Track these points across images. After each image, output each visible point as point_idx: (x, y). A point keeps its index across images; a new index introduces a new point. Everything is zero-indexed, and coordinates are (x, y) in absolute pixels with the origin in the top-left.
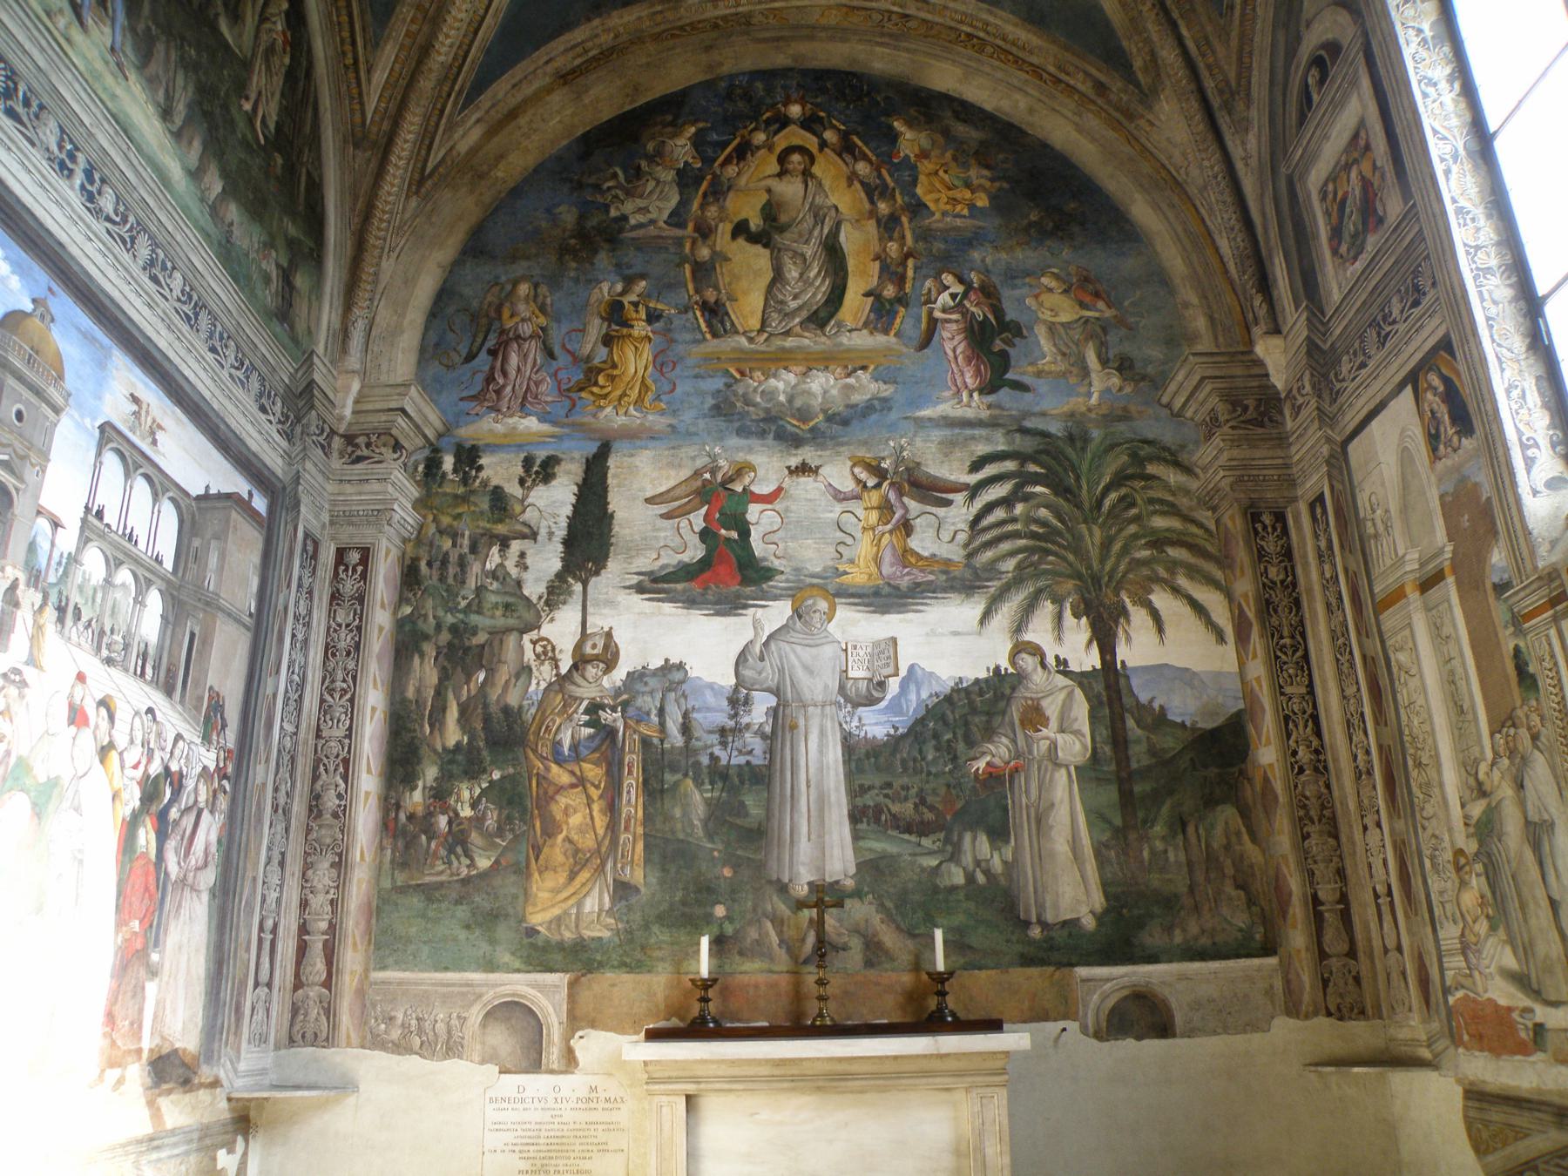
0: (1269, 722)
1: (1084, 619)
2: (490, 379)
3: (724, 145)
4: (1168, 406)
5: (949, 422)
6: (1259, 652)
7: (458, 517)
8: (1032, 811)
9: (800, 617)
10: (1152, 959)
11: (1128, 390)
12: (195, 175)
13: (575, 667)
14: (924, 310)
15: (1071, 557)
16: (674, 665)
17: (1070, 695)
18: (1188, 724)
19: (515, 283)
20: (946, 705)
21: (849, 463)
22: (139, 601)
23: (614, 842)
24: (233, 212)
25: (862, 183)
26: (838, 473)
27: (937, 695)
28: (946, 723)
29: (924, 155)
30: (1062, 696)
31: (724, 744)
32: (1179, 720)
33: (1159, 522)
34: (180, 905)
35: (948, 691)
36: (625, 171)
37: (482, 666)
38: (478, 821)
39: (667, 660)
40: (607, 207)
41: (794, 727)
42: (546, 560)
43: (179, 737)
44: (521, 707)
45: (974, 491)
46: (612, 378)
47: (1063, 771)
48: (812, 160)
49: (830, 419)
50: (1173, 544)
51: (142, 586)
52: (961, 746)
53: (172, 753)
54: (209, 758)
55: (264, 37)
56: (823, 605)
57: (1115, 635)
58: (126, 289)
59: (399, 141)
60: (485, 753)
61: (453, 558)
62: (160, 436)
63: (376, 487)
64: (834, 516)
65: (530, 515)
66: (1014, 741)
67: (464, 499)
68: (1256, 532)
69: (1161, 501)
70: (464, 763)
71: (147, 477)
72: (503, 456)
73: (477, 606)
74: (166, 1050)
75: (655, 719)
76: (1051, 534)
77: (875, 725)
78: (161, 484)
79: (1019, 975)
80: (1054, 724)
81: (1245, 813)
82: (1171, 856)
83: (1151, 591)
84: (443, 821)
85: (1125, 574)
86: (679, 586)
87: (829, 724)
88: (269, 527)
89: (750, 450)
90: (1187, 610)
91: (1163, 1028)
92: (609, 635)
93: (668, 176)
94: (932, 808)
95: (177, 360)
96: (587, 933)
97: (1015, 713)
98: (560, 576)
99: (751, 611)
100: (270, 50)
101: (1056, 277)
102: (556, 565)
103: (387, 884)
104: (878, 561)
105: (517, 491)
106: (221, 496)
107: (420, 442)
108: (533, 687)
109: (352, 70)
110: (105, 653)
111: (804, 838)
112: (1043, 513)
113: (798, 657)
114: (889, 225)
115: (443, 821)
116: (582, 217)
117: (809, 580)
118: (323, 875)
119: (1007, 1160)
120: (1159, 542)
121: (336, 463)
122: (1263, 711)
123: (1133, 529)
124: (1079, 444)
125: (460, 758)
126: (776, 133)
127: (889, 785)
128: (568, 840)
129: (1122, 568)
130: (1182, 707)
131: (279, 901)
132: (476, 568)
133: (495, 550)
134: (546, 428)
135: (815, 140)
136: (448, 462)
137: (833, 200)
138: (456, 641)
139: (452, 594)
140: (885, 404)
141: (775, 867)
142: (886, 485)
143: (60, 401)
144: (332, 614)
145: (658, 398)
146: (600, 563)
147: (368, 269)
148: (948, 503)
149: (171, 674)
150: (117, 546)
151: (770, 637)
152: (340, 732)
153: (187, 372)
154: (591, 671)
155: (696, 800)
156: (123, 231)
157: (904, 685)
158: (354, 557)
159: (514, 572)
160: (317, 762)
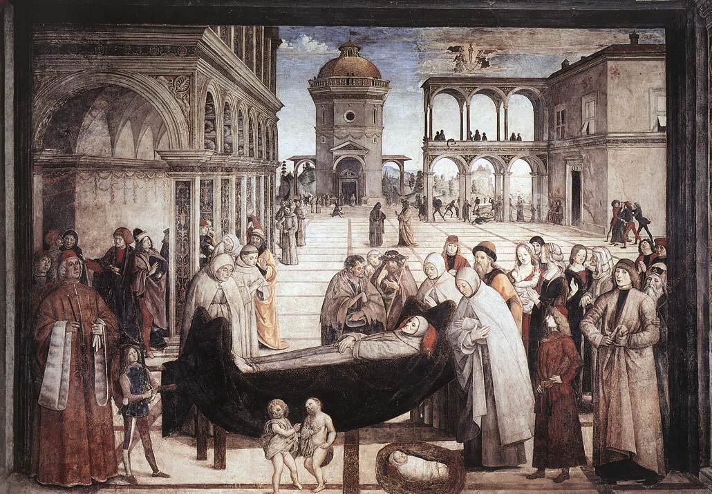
34: (611, 362)
53: (572, 261)
106: (584, 60)
110: (473, 217)
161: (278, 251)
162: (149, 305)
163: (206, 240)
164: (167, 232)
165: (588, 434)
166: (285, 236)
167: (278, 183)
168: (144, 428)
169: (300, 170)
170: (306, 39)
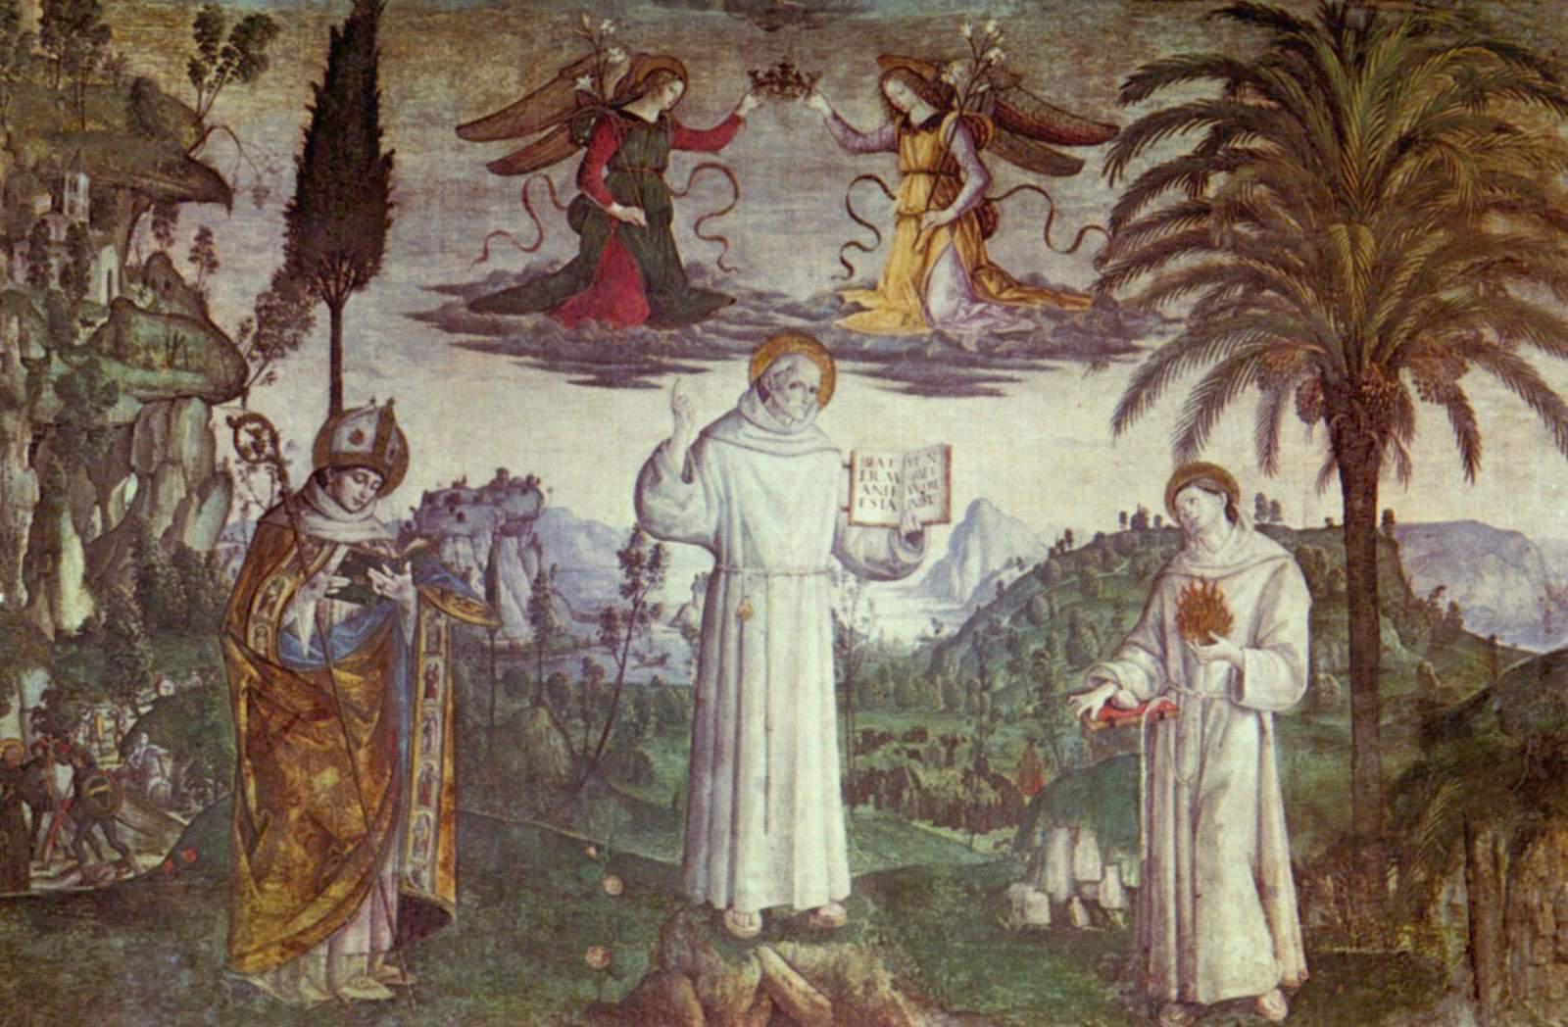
8: (1185, 792)
9: (764, 396)
13: (318, 477)
16: (514, 484)
20: (1038, 585)
21: (879, 71)
27: (1020, 563)
28: (1033, 620)
30: (1265, 572)
33: (1497, 225)
35: (1042, 556)
37: (132, 469)
39: (501, 472)
44: (211, 555)
47: (1251, 723)
56: (810, 372)
57: (1378, 460)
66: (1163, 659)
83: (1461, 370)
84: (63, 776)
86: (527, 321)
92: (386, 417)
94: (997, 782)
96: (349, 992)
99: (668, 380)
102: (275, 259)
108: (234, 518)
113: (756, 474)
115: (63, 776)
117: (783, 320)
125: (90, 652)
127: (919, 734)
128: (313, 818)
138: (72, 415)
141: (701, 882)
148: (1074, 167)
151: (705, 434)
154: (352, 488)
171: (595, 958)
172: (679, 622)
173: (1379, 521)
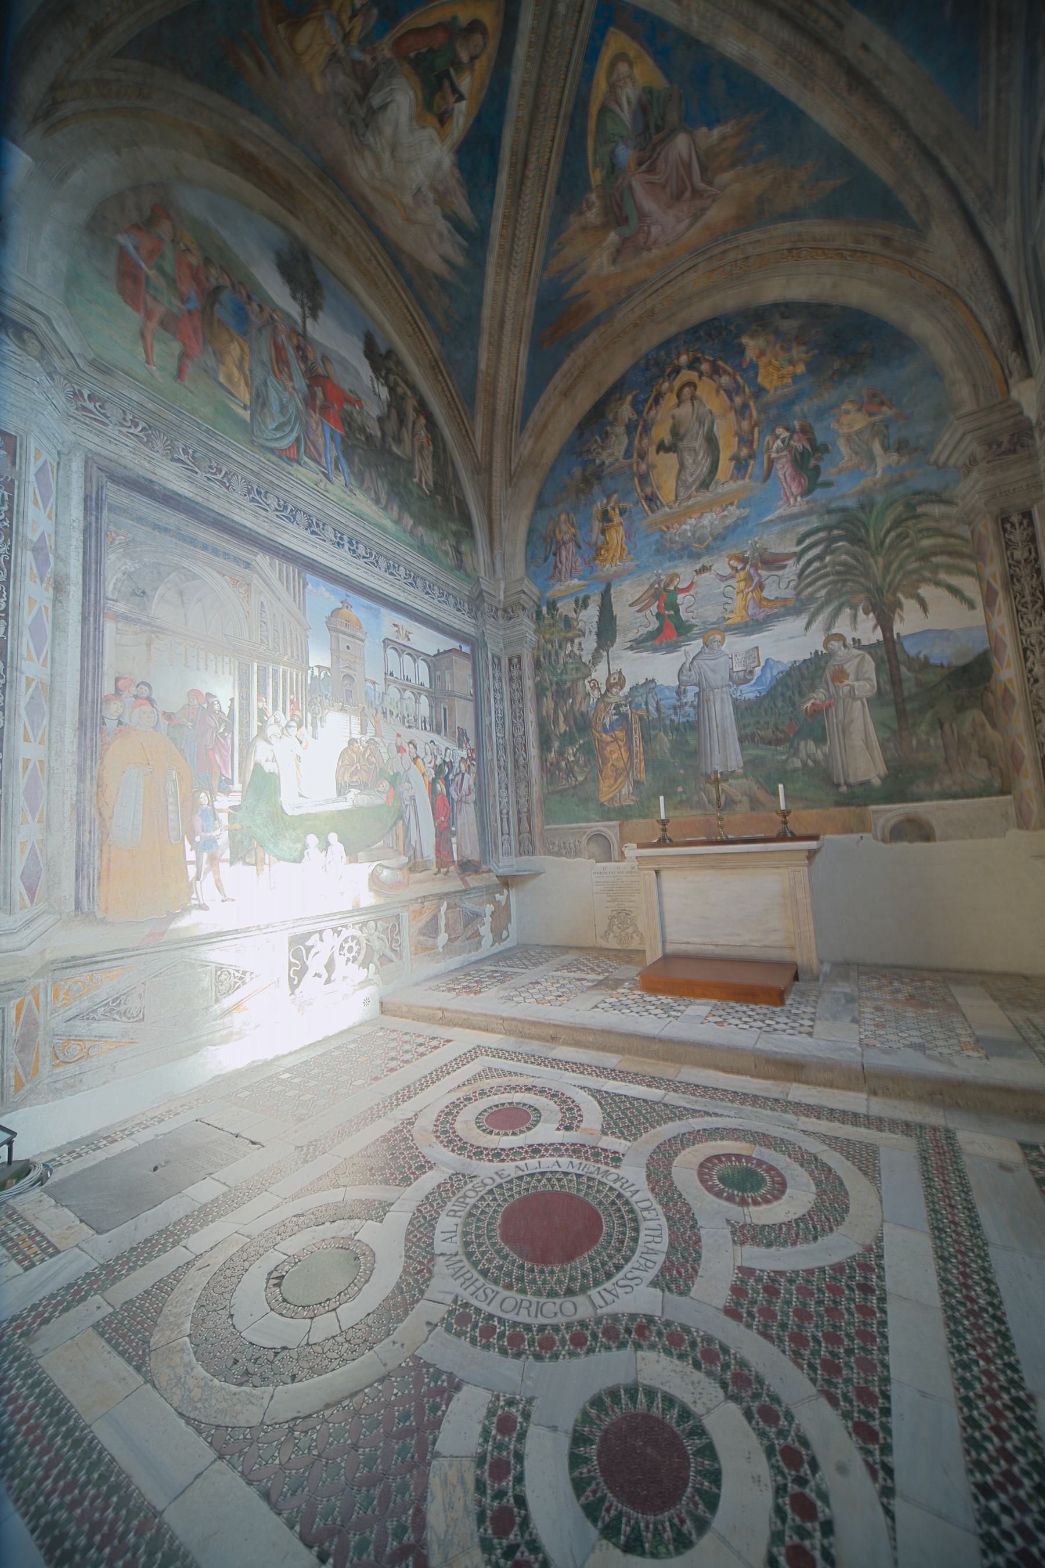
0: (1010, 652)
1: (871, 615)
2: (556, 566)
3: (646, 400)
4: (936, 463)
5: (782, 519)
6: (1003, 608)
7: (552, 634)
8: (840, 727)
10: (920, 799)
11: (904, 461)
12: (398, 522)
13: (607, 690)
14: (765, 457)
15: (862, 580)
17: (863, 659)
18: (945, 664)
19: (559, 516)
22: (417, 701)
23: (632, 764)
24: (421, 530)
25: (726, 391)
26: (721, 566)
29: (762, 354)
30: (857, 660)
31: (676, 714)
32: (938, 662)
33: (926, 543)
36: (600, 437)
38: (576, 762)
40: (594, 460)
41: (708, 701)
42: (590, 643)
43: (447, 748)
45: (799, 556)
46: (607, 550)
47: (859, 702)
48: (695, 387)
49: (715, 539)
50: (936, 554)
51: (417, 696)
52: (797, 697)
54: (464, 754)
55: (417, 444)
56: (718, 637)
58: (380, 583)
59: (494, 464)
60: (577, 735)
61: (553, 652)
62: (410, 636)
63: (518, 628)
64: (721, 590)
65: (581, 625)
66: (828, 691)
67: (554, 625)
68: (1005, 530)
69: (928, 529)
70: (568, 739)
71: (409, 654)
72: (566, 601)
73: (565, 671)
74: (465, 860)
75: (643, 706)
76: (848, 568)
77: (749, 692)
78: (416, 655)
79: (834, 811)
80: (852, 677)
81: (988, 713)
82: (932, 742)
83: (919, 587)
84: (563, 764)
85: (899, 582)
86: (649, 644)
87: (725, 696)
88: (473, 658)
89: (676, 567)
90: (945, 593)
91: (927, 836)
92: (620, 672)
93: (620, 430)
94: (782, 732)
95: (411, 604)
96: (624, 803)
97: (828, 674)
98: (597, 650)
99: (683, 648)
100: (421, 448)
101: (852, 402)
103: (546, 791)
104: (746, 608)
105: (574, 616)
106: (445, 652)
107: (532, 603)
109: (465, 435)
111: (717, 752)
112: (844, 557)
114: (742, 412)
115: (563, 764)
116: (584, 470)
118: (523, 791)
119: (809, 901)
120: (925, 556)
121: (501, 621)
122: (1005, 646)
123: (906, 552)
124: (867, 509)
126: (674, 379)
127: (758, 723)
129: (898, 577)
130: (942, 654)
131: (508, 802)
132: (562, 654)
133: (569, 645)
134: (582, 582)
135: (696, 374)
136: (544, 609)
137: (708, 407)
139: (555, 668)
140: (745, 519)
142: (748, 567)
143: (363, 637)
144: (511, 686)
145: (629, 553)
146: (613, 641)
147: (496, 530)
149: (438, 727)
150: (402, 684)
151: (694, 659)
152: (521, 734)
153: (417, 607)
154: (614, 690)
155: (665, 740)
156: (372, 559)
157: (763, 670)
158: (515, 660)
159: (577, 652)
160: (515, 747)
161: (310, 728)
162: (217, 757)
163: (262, 712)
164: (232, 700)
165: (454, 847)
166: (314, 718)
167: (309, 682)
168: (213, 860)
169: (322, 676)
170: (323, 589)
171: (680, 789)
172: (692, 706)
173: (895, 636)
